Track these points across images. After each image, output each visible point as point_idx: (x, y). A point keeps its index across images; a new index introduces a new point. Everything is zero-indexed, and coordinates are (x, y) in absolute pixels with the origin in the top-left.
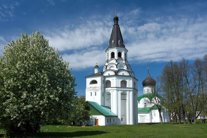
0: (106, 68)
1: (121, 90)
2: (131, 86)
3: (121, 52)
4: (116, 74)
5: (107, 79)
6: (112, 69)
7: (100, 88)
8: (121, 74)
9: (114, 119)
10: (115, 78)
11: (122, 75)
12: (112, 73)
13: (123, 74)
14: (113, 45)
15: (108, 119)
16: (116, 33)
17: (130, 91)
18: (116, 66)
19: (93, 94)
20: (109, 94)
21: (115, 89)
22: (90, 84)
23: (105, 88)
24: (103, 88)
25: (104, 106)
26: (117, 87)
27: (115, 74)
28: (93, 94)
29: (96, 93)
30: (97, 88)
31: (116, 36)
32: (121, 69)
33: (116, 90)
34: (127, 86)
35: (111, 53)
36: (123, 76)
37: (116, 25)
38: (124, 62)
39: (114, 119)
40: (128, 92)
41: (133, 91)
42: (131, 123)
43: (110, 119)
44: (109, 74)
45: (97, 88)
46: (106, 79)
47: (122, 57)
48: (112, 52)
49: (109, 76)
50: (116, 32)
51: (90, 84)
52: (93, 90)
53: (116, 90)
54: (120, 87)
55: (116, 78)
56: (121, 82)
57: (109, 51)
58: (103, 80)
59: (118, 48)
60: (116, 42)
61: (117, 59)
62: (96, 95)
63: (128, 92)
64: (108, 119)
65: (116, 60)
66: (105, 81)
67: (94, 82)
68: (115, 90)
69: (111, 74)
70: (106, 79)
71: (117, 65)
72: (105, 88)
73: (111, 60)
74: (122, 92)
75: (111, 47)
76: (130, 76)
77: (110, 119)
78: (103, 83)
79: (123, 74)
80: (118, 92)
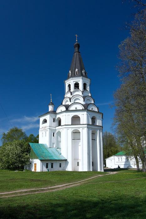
2: (85, 122)
8: (72, 108)
9: (60, 164)
11: (75, 109)
12: (64, 109)
15: (47, 164)
20: (59, 133)
32: (77, 101)
33: (65, 128)
36: (76, 110)
38: (80, 93)
39: (60, 164)
40: (80, 130)
42: (86, 169)
43: (52, 164)
45: (46, 128)
49: (62, 112)
52: (43, 131)
64: (47, 164)
67: (45, 121)
74: (72, 130)
76: (85, 109)
77: (52, 164)
79: (76, 108)
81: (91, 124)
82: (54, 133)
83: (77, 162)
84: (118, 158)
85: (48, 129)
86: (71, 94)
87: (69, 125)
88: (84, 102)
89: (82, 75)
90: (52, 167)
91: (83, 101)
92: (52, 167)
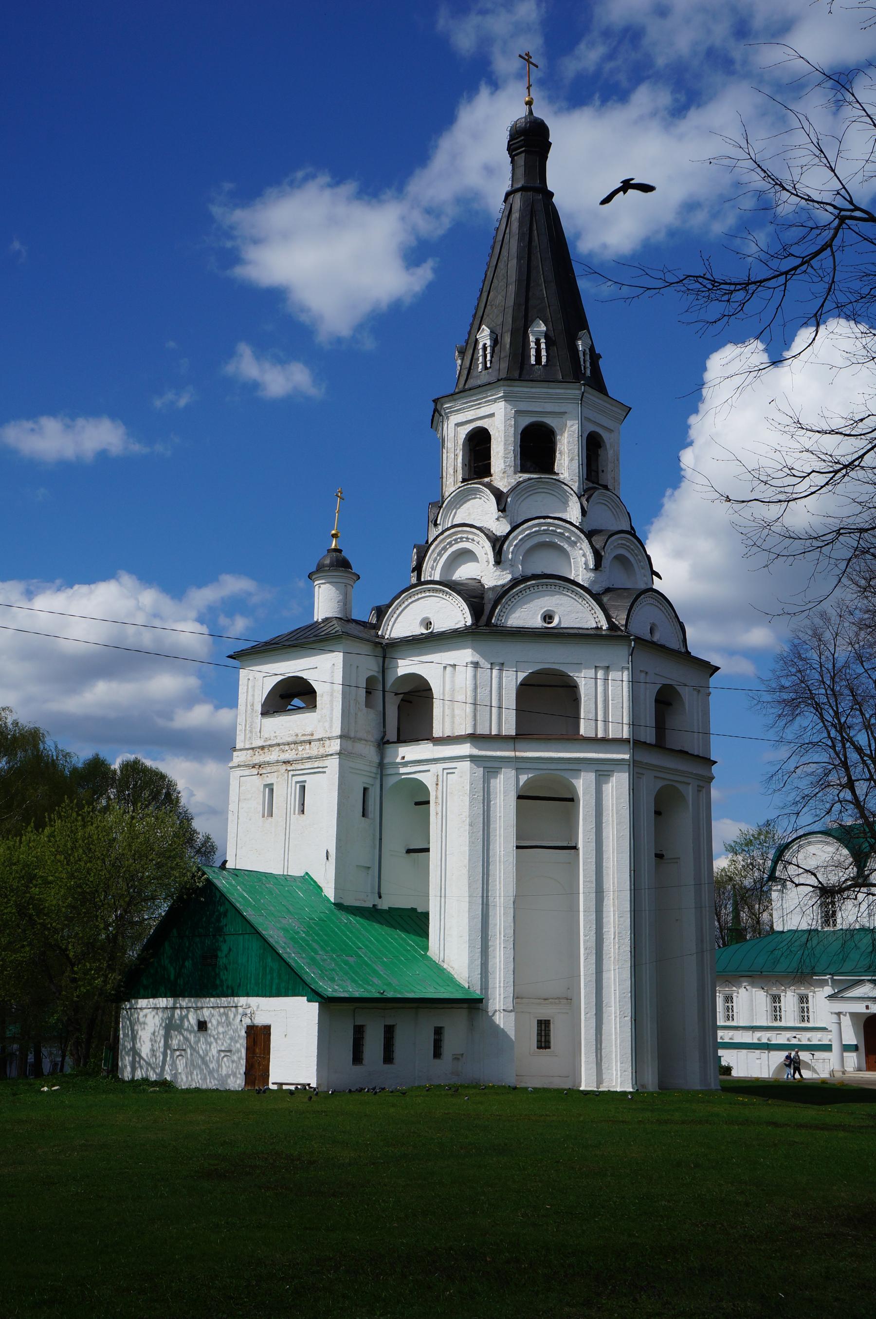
0: (418, 568)
1: (519, 765)
3: (549, 421)
4: (484, 618)
5: (405, 666)
6: (464, 573)
7: (335, 746)
9: (438, 1031)
10: (465, 655)
11: (537, 622)
13: (548, 617)
14: (486, 368)
15: (359, 1033)
16: (513, 263)
17: (603, 770)
18: (488, 546)
19: (285, 793)
21: (466, 749)
22: (265, 713)
23: (383, 743)
24: (370, 752)
25: (373, 914)
26: (482, 730)
27: (469, 623)
28: (285, 793)
29: (303, 788)
30: (314, 750)
31: (512, 288)
32: (544, 564)
33: (473, 758)
34: (584, 730)
35: (461, 441)
37: (521, 189)
41: (636, 769)
43: (389, 1033)
44: (428, 624)
46: (401, 662)
47: (556, 470)
48: (469, 428)
50: (519, 258)
51: (265, 713)
52: (284, 767)
53: (473, 758)
54: (509, 728)
55: (477, 658)
56: (525, 689)
57: (454, 419)
58: (370, 681)
59: (521, 389)
60: (507, 339)
61: (513, 489)
62: (303, 812)
63: (592, 776)
64: (359, 1033)
65: (499, 496)
66: (390, 681)
68: (466, 765)
69: (441, 625)
70: (401, 662)
71: (498, 543)
72: (383, 743)
73: (462, 498)
74: (523, 778)
75: (472, 383)
76: (612, 626)
77: (389, 1033)
78: (368, 704)
79: (548, 617)
80: (486, 782)
81: (650, 736)
82: (365, 790)
83: (540, 1022)
84: (796, 999)
85: (333, 764)
86: (502, 508)
87: (499, 739)
88: (591, 575)
89: (574, 374)
90: (388, 1058)
91: (591, 565)
92: (388, 1058)
